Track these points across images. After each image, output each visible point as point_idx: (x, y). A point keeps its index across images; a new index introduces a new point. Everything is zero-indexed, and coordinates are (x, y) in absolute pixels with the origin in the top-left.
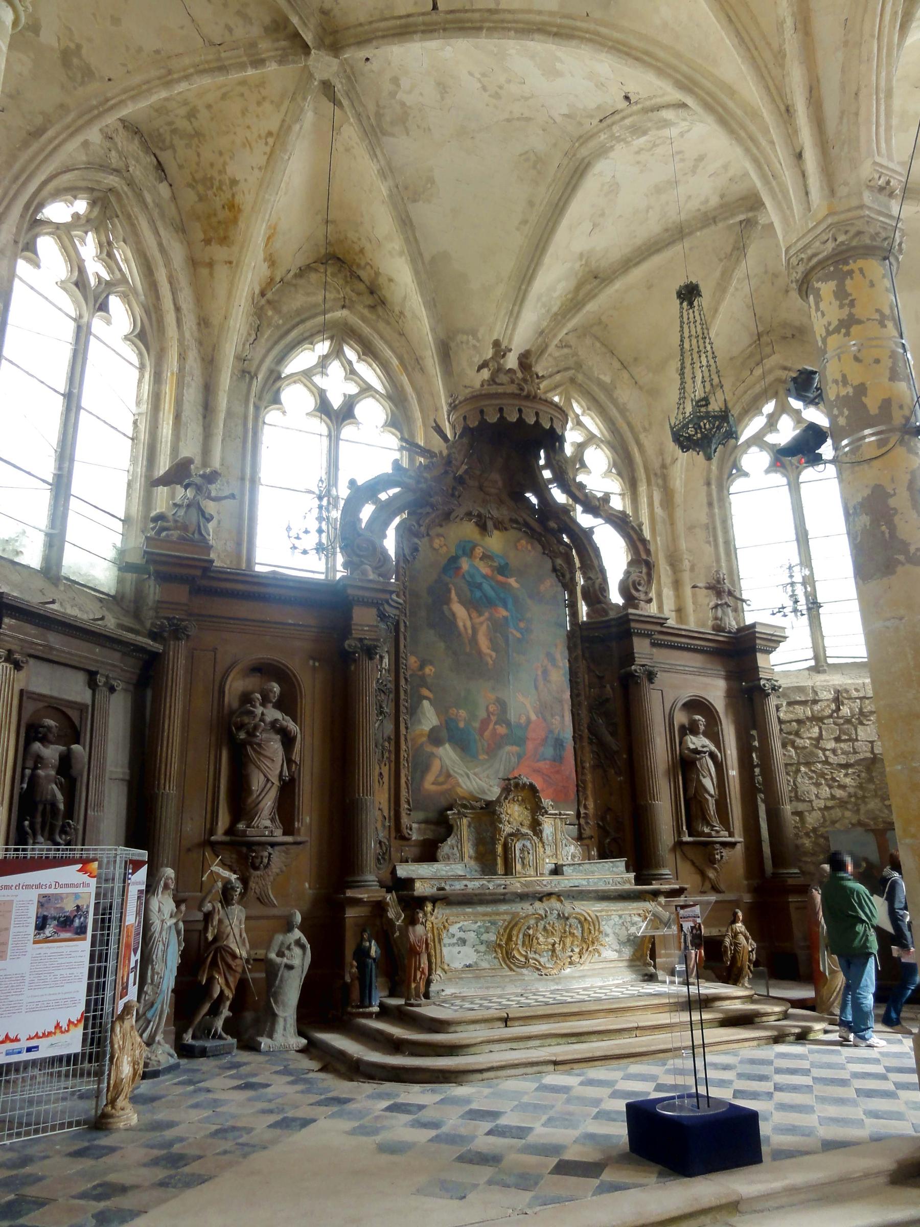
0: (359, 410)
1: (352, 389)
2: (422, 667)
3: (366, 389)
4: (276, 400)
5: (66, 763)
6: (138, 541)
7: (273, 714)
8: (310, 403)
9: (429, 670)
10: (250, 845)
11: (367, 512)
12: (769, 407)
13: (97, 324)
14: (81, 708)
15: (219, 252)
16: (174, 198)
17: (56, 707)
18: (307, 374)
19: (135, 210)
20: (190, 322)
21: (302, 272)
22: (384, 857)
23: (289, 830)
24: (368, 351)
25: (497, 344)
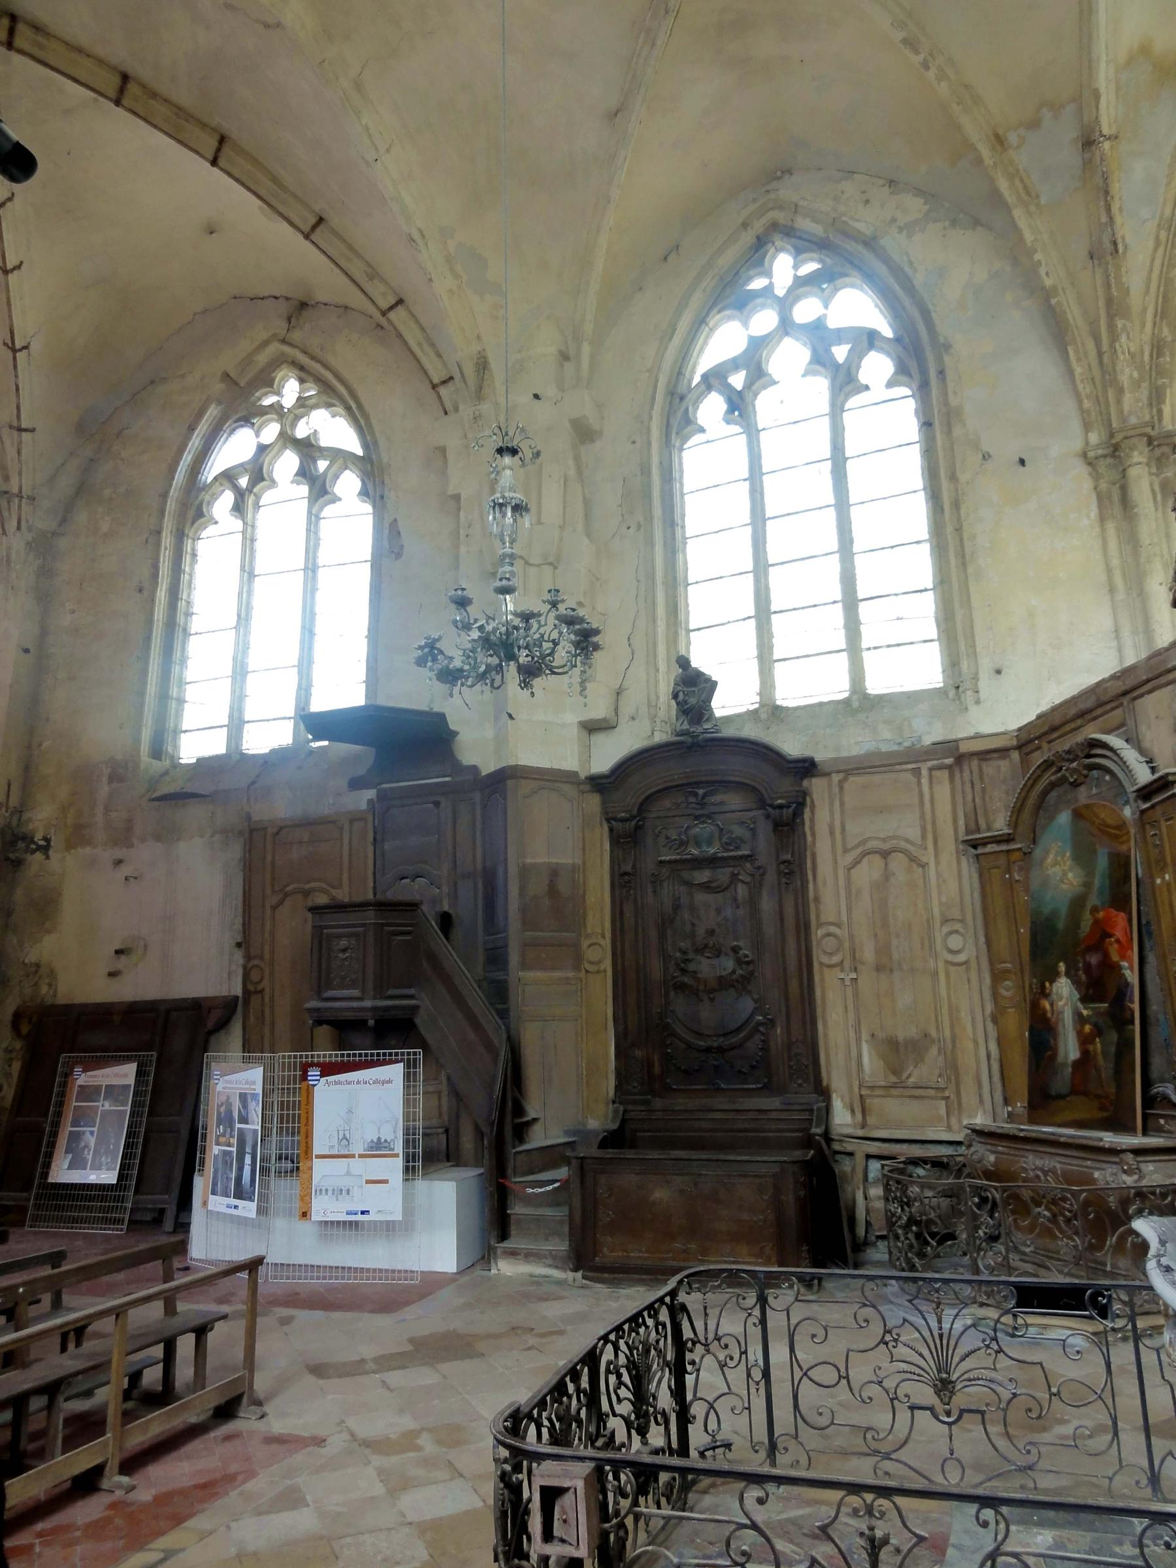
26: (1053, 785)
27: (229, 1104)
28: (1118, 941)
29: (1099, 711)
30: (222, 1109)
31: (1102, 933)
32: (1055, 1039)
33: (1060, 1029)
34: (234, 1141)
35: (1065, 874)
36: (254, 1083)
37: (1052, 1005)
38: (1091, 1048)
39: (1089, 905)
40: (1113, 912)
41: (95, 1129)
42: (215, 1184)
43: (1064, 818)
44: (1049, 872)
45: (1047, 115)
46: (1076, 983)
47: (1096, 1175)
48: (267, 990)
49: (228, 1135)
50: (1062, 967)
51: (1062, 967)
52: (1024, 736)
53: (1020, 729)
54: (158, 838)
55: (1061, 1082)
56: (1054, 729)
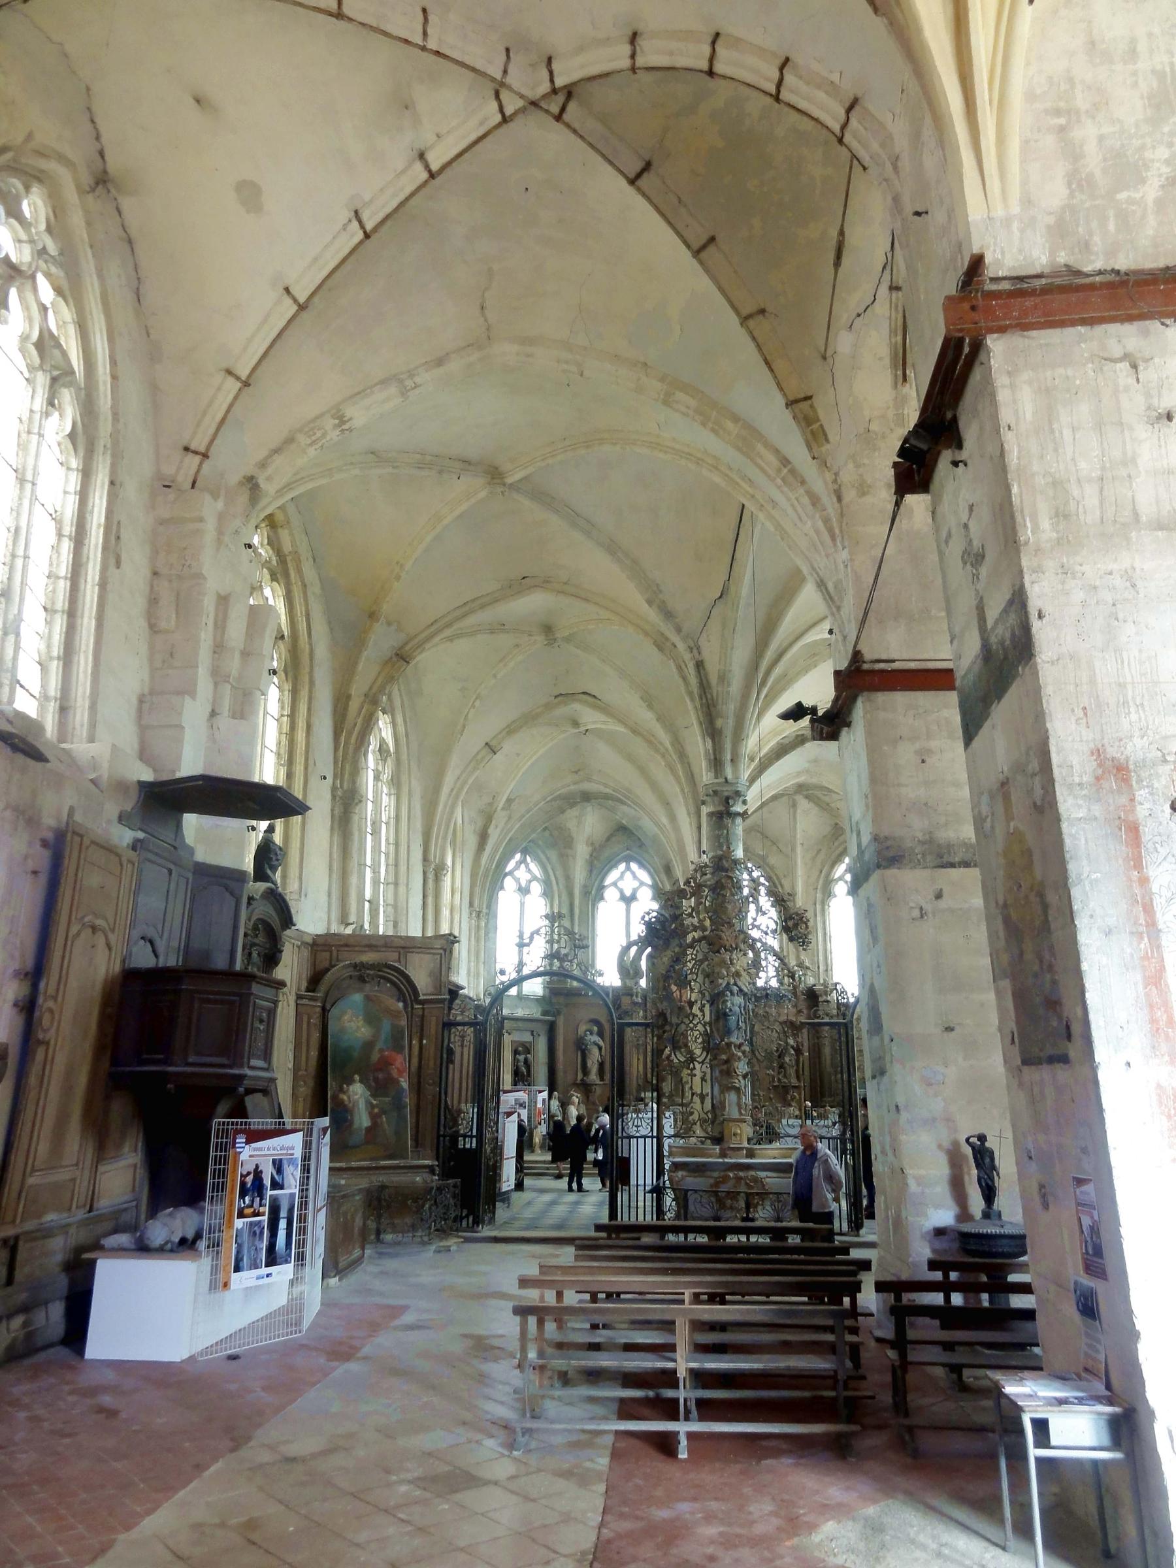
0: (638, 895)
1: (636, 884)
3: (642, 884)
4: (602, 898)
5: (526, 1061)
7: (595, 1038)
8: (618, 895)
14: (530, 1043)
15: (569, 852)
16: (551, 835)
17: (523, 1044)
18: (615, 884)
20: (562, 881)
21: (608, 839)
23: (602, 1079)
24: (642, 865)
26: (351, 977)
27: (258, 1174)
28: (398, 1069)
30: (249, 1179)
31: (385, 1063)
32: (352, 1115)
34: (266, 1209)
35: (358, 1027)
36: (292, 1148)
37: (349, 1098)
38: (379, 1120)
39: (377, 1048)
40: (394, 1053)
43: (357, 998)
44: (347, 1025)
46: (368, 1087)
47: (418, 1179)
48: (52, 1042)
49: (256, 1205)
50: (357, 1077)
51: (357, 1077)
52: (320, 941)
53: (317, 935)
55: (358, 1138)
56: (347, 945)
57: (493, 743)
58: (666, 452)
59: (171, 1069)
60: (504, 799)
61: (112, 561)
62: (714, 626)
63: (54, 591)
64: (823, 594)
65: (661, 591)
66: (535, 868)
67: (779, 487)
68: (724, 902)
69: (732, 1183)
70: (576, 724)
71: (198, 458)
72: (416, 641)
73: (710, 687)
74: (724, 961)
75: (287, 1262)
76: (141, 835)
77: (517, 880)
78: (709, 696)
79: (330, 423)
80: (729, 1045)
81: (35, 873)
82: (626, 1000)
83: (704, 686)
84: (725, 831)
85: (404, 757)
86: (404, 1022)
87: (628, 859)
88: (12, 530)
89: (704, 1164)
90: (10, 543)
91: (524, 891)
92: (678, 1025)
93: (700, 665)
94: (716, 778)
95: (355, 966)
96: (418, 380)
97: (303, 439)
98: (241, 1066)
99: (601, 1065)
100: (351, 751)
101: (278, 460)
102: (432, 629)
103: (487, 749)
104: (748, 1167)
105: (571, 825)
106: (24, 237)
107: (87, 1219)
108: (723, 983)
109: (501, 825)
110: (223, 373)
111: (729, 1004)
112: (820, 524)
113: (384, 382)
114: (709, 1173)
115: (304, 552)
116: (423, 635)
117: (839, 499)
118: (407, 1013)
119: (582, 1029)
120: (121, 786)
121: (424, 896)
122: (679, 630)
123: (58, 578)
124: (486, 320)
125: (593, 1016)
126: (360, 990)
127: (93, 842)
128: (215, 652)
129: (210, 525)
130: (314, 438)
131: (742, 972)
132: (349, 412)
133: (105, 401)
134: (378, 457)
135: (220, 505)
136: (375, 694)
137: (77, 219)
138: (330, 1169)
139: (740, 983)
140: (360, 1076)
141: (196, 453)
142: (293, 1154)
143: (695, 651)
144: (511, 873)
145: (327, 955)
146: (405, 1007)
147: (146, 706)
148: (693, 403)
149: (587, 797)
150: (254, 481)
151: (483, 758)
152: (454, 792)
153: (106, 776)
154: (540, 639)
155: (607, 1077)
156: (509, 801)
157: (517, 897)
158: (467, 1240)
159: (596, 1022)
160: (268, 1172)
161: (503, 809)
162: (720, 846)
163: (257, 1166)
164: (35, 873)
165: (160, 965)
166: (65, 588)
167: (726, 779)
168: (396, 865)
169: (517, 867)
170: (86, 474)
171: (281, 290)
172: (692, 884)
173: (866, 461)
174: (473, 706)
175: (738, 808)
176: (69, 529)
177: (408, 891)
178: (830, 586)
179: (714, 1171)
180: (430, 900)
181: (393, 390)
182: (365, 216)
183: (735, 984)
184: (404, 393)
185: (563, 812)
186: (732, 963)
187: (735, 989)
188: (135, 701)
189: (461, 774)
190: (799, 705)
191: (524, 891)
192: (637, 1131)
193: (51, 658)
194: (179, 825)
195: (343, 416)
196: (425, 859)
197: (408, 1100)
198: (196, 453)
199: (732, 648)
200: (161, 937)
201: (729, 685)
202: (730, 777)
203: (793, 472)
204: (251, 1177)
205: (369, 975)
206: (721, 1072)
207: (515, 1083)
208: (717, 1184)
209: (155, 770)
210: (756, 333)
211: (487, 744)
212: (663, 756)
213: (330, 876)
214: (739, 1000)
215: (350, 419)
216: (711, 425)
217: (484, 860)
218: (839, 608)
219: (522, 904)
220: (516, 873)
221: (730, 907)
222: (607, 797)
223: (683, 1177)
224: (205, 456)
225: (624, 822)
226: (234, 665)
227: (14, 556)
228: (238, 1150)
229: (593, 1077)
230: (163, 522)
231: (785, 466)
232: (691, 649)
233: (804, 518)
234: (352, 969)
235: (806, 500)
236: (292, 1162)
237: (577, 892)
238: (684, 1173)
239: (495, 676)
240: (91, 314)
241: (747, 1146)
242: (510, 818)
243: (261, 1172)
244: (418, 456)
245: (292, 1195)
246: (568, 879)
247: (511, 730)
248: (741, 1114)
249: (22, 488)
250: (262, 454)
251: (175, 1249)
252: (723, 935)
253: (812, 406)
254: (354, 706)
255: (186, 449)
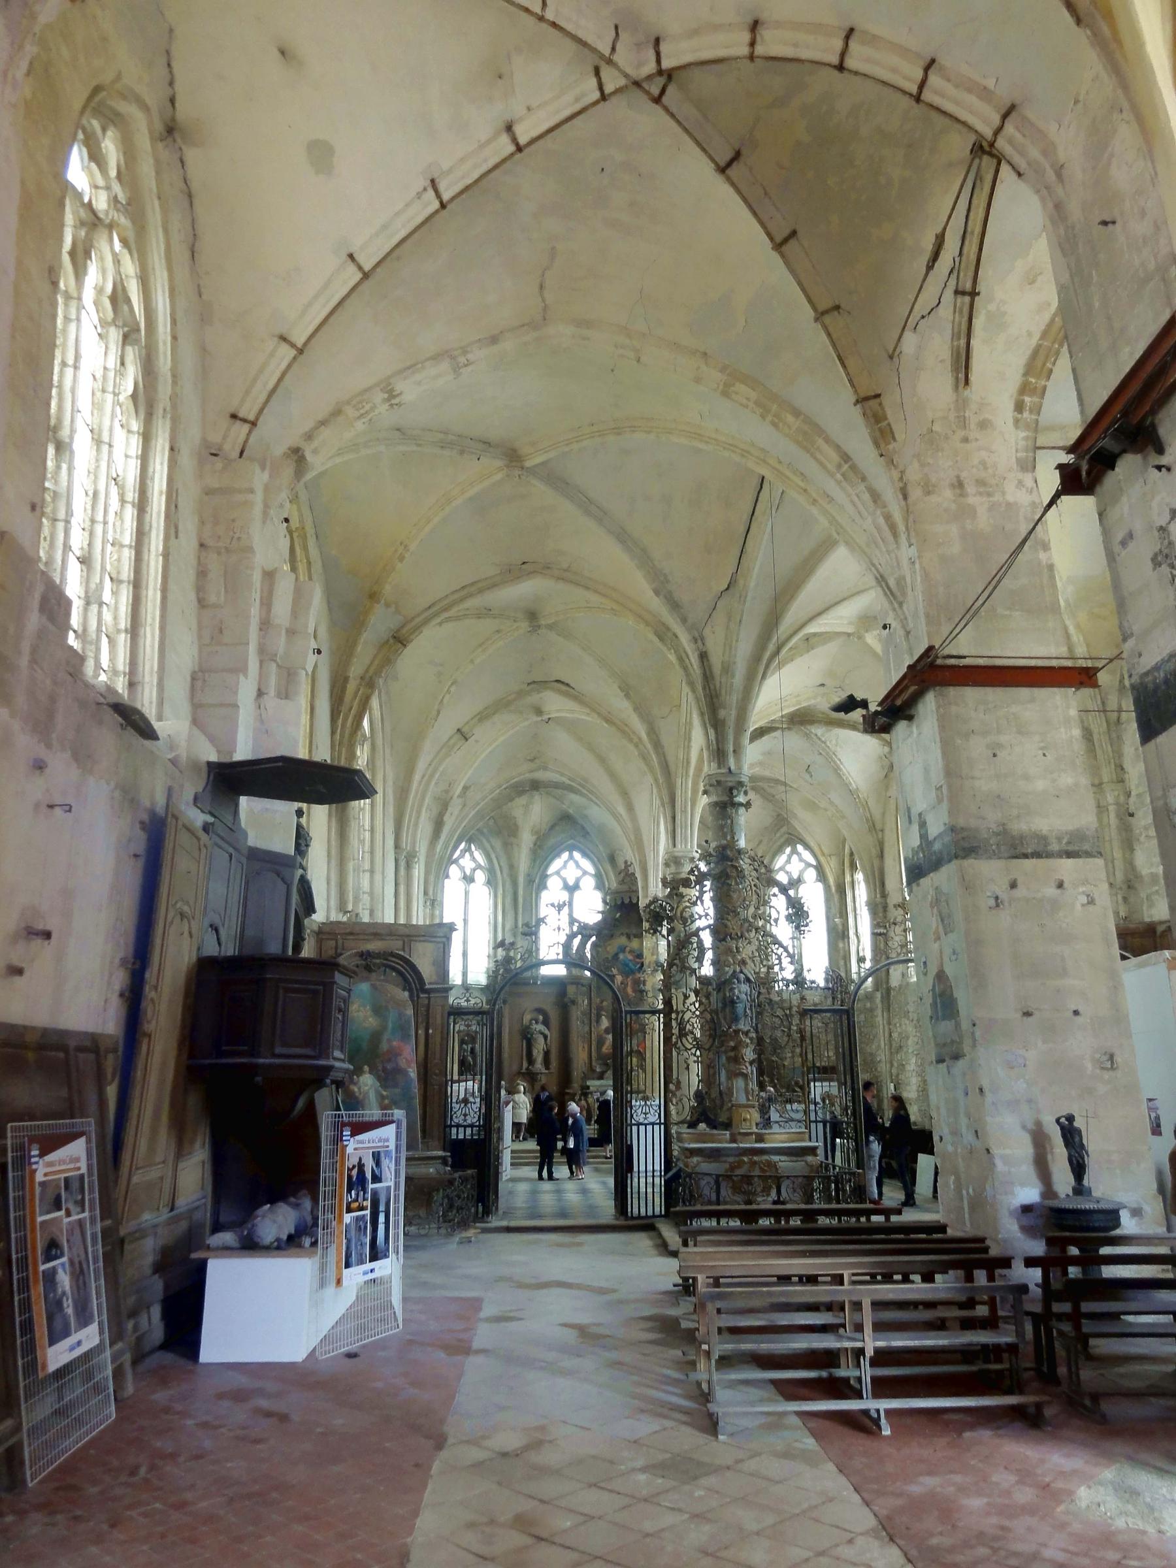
0: (581, 884)
1: (579, 873)
2: (602, 1002)
3: (585, 873)
4: (545, 887)
6: (492, 965)
7: (541, 1027)
8: (561, 885)
9: (605, 1003)
10: (533, 1074)
11: (576, 942)
12: (788, 850)
13: (472, 884)
18: (558, 873)
19: (482, 838)
20: (506, 870)
21: (552, 827)
22: (586, 1077)
23: (547, 1068)
24: (585, 855)
25: (626, 862)
27: (361, 1166)
29: (388, 938)
30: (355, 1172)
33: (367, 1101)
34: (368, 1203)
37: (359, 1089)
41: (64, 1259)
42: (348, 1256)
44: (355, 1014)
45: (393, 609)
46: (379, 1078)
49: (360, 1199)
50: (366, 1068)
51: (366, 1068)
52: (327, 929)
53: (323, 923)
54: (76, 757)
56: (351, 934)
57: (464, 730)
58: (707, 442)
59: (261, 1061)
60: (460, 788)
61: (172, 531)
62: (720, 617)
63: (119, 560)
64: (884, 590)
65: (668, 581)
66: (478, 855)
67: (839, 483)
68: (729, 890)
69: (746, 1167)
70: (539, 711)
71: (246, 427)
72: (413, 624)
73: (713, 678)
74: (731, 951)
75: (386, 1256)
76: (211, 819)
77: (462, 869)
78: (712, 687)
79: (379, 397)
80: (737, 1032)
81: (136, 856)
82: (571, 990)
83: (707, 676)
84: (729, 821)
85: (379, 742)
86: (410, 1012)
87: (571, 849)
88: (91, 493)
89: (718, 1150)
90: (89, 507)
91: (469, 879)
92: (684, 1013)
93: (703, 656)
94: (719, 767)
95: (361, 954)
96: (470, 356)
97: (350, 412)
98: (328, 1058)
99: (547, 1054)
100: (347, 732)
101: (325, 433)
102: (431, 611)
103: (459, 736)
104: (762, 1151)
105: (518, 813)
106: (101, 182)
107: (172, 1218)
108: (729, 971)
109: (456, 813)
110: (276, 339)
111: (736, 991)
112: (881, 521)
113: (436, 358)
114: (724, 1159)
115: (310, 531)
116: (418, 620)
117: (905, 497)
118: (412, 1001)
119: (527, 1018)
120: (194, 765)
121: (396, 884)
122: (684, 620)
123: (122, 546)
124: (544, 301)
125: (536, 1006)
126: (367, 979)
127: (184, 826)
128: (261, 629)
129: (258, 497)
130: (362, 411)
131: (748, 961)
132: (399, 386)
133: (164, 363)
134: (404, 434)
135: (265, 476)
136: (371, 678)
137: (146, 168)
138: (408, 1159)
139: (745, 971)
140: (369, 1066)
141: (245, 421)
142: (388, 1147)
143: (700, 642)
144: (456, 861)
145: (333, 943)
146: (411, 997)
147: (199, 683)
148: (753, 395)
149: (535, 785)
150: (300, 453)
151: (454, 745)
152: (426, 778)
153: (184, 755)
154: (524, 625)
155: (554, 1064)
156: (466, 788)
157: (461, 885)
158: (485, 1231)
159: (540, 1011)
160: (369, 1164)
161: (459, 796)
162: (725, 837)
163: (360, 1159)
164: (136, 856)
165: (223, 954)
166: (130, 558)
167: (730, 769)
168: (372, 852)
169: (462, 856)
170: (147, 437)
171: (344, 257)
172: (696, 873)
173: (930, 461)
174: (448, 691)
175: (741, 799)
176: (131, 495)
177: (383, 881)
178: (892, 582)
179: (728, 1156)
180: (402, 888)
181: (445, 366)
182: (442, 187)
183: (741, 972)
184: (456, 369)
185: (512, 800)
186: (738, 951)
187: (742, 976)
188: (189, 679)
189: (432, 761)
190: (851, 697)
191: (469, 879)
192: (645, 1119)
193: (119, 631)
194: (237, 805)
195: (392, 390)
196: (397, 846)
197: (416, 1089)
198: (245, 421)
199: (737, 641)
200: (223, 925)
201: (733, 676)
202: (733, 768)
203: (854, 468)
204: (356, 1170)
205: (375, 964)
206: (728, 1059)
207: (461, 1073)
208: (732, 1168)
209: (219, 752)
210: (831, 329)
211: (458, 730)
212: (636, 746)
213: (329, 862)
214: (745, 987)
215: (401, 394)
216: (769, 418)
217: (439, 848)
218: (901, 604)
219: (467, 893)
220: (461, 861)
221: (735, 896)
222: (557, 785)
223: (698, 1163)
224: (254, 424)
225: (571, 811)
226: (280, 643)
227: (93, 521)
228: (345, 1143)
229: (539, 1065)
230: (209, 492)
231: (846, 462)
232: (696, 641)
233: (865, 514)
234: (357, 958)
235: (866, 496)
236: (388, 1153)
237: (521, 880)
238: (699, 1159)
239: (472, 661)
240: (153, 269)
241: (756, 1131)
242: (464, 805)
243: (364, 1165)
244: (442, 436)
245: (389, 1188)
246: (512, 867)
247: (483, 717)
248: (748, 1100)
249: (98, 450)
250: (308, 425)
251: (283, 1245)
252: (729, 923)
253: (880, 404)
254: (351, 687)
255: (234, 416)
